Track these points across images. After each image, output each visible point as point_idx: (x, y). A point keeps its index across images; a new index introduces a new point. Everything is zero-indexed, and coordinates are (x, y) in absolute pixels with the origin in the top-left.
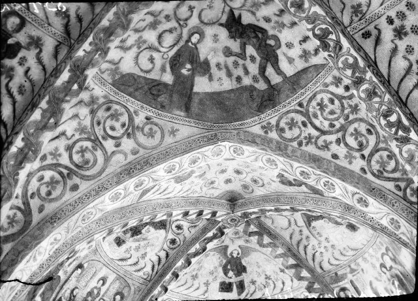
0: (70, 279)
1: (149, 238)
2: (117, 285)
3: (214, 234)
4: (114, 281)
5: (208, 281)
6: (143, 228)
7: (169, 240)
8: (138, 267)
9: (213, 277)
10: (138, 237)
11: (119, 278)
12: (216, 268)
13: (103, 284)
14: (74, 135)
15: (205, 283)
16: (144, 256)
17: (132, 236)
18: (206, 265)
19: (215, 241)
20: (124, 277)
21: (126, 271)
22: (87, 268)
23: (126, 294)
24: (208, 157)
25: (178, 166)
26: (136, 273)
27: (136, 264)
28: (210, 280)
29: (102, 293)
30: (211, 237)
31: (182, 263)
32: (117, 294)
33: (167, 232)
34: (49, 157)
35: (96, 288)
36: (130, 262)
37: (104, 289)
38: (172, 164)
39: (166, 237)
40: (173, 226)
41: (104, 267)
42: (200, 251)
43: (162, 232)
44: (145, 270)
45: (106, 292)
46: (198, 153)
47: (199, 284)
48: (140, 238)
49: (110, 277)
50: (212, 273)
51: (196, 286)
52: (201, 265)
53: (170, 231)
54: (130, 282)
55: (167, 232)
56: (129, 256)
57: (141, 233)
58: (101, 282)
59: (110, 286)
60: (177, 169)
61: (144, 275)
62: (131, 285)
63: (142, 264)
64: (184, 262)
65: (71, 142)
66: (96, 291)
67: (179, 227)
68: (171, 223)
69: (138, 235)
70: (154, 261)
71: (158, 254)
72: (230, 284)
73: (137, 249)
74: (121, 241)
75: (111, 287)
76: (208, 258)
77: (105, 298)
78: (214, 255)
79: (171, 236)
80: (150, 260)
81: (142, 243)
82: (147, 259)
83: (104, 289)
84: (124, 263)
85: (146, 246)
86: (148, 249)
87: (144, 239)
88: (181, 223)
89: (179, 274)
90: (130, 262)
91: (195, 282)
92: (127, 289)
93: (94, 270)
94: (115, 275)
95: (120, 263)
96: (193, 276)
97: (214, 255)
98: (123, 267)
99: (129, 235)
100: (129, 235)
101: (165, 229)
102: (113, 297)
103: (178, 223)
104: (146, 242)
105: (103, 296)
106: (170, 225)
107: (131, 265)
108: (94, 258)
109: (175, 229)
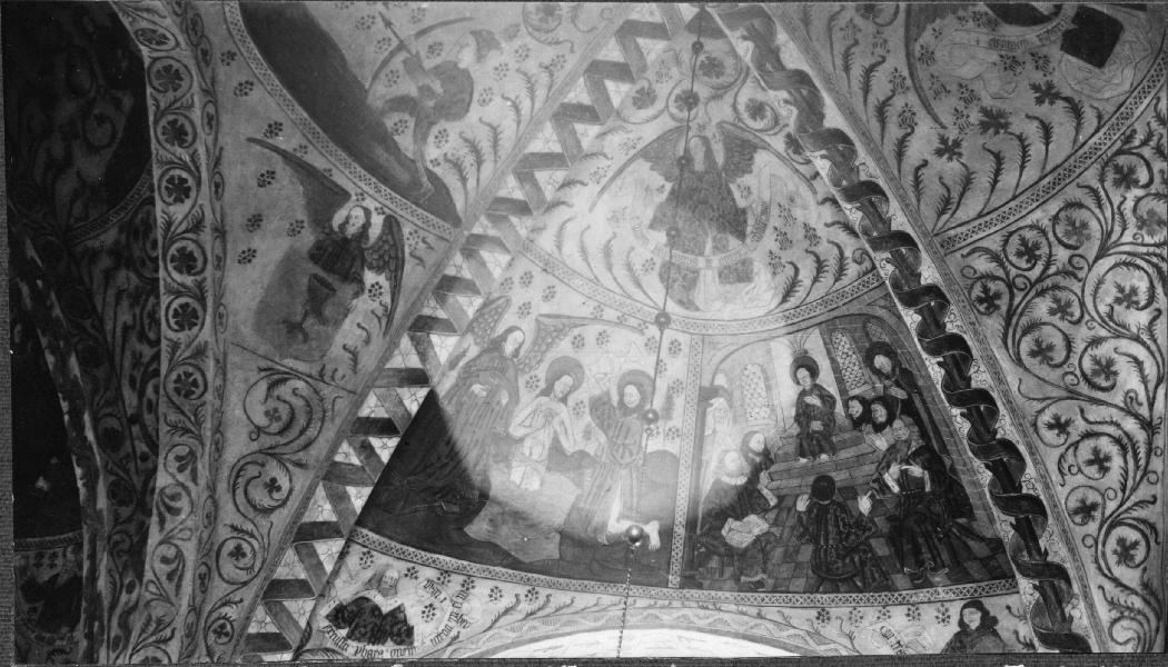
0: (708, 432)
1: (766, 196)
2: (844, 343)
3: (745, 38)
5: (1036, 88)
6: (733, 200)
7: (790, 151)
8: (832, 264)
9: (1030, 66)
10: (751, 221)
11: (829, 328)
12: (994, 44)
13: (814, 371)
14: (134, 315)
15: (1040, 101)
16: (811, 235)
18: (968, 71)
19: (782, 37)
20: (835, 313)
21: (824, 301)
22: (730, 380)
23: (886, 339)
24: (175, 101)
25: (177, 172)
26: (845, 280)
27: (820, 266)
28: (1039, 78)
29: (833, 390)
30: (757, 46)
31: (823, 157)
32: (868, 360)
33: (766, 147)
34: (135, 373)
35: (803, 394)
36: (806, 275)
37: (827, 379)
38: (164, 184)
39: (778, 155)
40: (751, 123)
41: (772, 344)
42: (804, 92)
43: (761, 158)
44: (848, 253)
45: (840, 380)
46: (156, 122)
47: (1028, 117)
48: (758, 221)
49: (807, 346)
50: (1011, 64)
51: (1032, 130)
52: (953, 88)
53: (767, 139)
54: (854, 309)
55: (766, 147)
56: (790, 271)
57: (744, 212)
58: (803, 373)
59: (833, 361)
60: (184, 175)
61: (860, 263)
62: (869, 311)
63: (825, 250)
64: (824, 152)
65: (138, 328)
66: (814, 400)
67: (757, 110)
68: (741, 124)
69: (745, 222)
70: (836, 219)
71: (820, 197)
73: (785, 241)
74: (740, 268)
75: (840, 361)
76: (938, 55)
77: (854, 392)
78: (938, 34)
79: (778, 143)
80: (827, 225)
81: (775, 220)
82: (822, 232)
83: (827, 379)
84: (800, 293)
85: (788, 217)
86: (798, 213)
87: (766, 210)
88: (743, 99)
89: (863, 177)
90: (806, 275)
91: (1015, 129)
92: (873, 328)
93: (757, 370)
94: (816, 332)
95: (793, 301)
96: (984, 127)
97: (938, 34)
98: (808, 300)
101: (755, 148)
102: (868, 372)
103: (741, 108)
104: (775, 211)
105: (843, 391)
106: (747, 129)
107: (816, 280)
108: (720, 355)
109: (759, 125)
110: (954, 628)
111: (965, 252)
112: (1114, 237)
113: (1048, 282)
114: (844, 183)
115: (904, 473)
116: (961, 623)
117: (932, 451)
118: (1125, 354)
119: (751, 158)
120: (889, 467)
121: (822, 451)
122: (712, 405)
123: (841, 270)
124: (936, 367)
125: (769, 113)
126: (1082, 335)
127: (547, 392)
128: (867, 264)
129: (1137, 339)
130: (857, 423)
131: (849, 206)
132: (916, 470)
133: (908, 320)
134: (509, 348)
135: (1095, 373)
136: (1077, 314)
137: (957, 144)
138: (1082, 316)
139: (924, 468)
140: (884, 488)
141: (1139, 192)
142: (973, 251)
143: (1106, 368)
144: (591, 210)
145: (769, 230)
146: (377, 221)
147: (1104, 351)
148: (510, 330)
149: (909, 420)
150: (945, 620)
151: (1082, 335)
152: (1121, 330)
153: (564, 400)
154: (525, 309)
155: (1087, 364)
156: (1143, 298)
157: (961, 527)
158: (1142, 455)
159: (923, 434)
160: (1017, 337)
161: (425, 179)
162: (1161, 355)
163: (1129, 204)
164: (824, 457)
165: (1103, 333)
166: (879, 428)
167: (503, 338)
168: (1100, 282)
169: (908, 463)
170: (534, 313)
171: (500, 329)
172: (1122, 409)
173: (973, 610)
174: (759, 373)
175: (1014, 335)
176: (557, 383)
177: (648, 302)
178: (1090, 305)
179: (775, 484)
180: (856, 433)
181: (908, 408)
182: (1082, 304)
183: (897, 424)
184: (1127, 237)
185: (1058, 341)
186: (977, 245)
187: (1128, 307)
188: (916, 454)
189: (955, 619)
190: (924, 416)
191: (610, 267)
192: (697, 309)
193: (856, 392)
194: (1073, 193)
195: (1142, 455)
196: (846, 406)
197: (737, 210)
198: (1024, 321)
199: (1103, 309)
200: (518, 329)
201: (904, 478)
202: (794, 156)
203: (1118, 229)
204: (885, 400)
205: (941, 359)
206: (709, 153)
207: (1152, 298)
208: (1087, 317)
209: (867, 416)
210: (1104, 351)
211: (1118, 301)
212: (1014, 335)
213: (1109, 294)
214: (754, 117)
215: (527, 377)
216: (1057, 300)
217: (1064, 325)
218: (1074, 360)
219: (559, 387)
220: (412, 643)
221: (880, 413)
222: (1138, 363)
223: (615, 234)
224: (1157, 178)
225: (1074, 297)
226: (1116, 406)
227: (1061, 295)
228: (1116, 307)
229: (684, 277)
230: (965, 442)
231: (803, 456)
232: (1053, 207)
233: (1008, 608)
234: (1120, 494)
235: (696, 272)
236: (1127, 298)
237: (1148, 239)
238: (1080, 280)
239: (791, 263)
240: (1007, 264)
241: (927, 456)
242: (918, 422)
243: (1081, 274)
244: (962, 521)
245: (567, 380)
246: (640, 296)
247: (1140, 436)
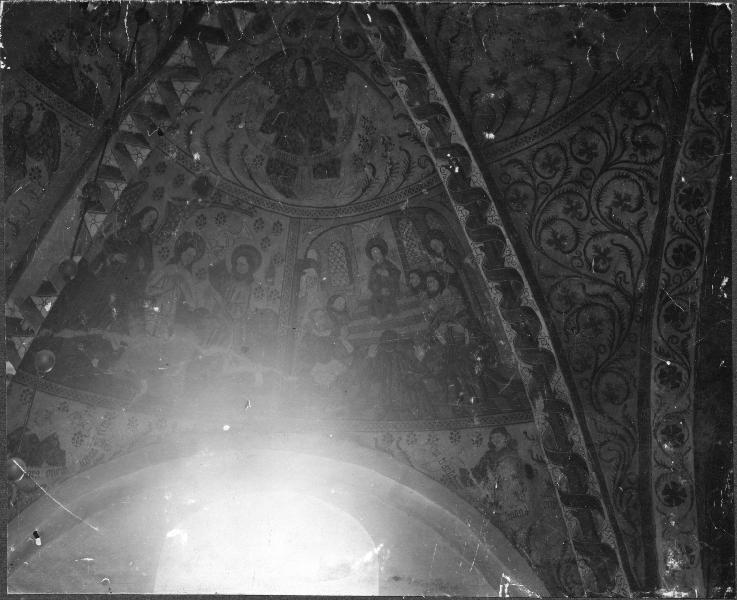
2: (407, 228)
4: (396, 228)
13: (384, 250)
17: (332, 139)
32: (426, 243)
35: (377, 267)
40: (347, 52)
43: (353, 78)
44: (415, 159)
58: (376, 251)
59: (399, 242)
81: (359, 131)
86: (379, 125)
87: (352, 120)
89: (432, 101)
90: (382, 176)
99: (326, 144)
100: (326, 144)
105: (405, 265)
110: (484, 448)
111: (505, 161)
112: (616, 156)
113: (565, 187)
114: (417, 104)
115: (450, 330)
116: (491, 445)
118: (617, 245)
119: (344, 78)
120: (439, 325)
121: (388, 312)
122: (305, 273)
123: (408, 171)
124: (479, 251)
125: (361, 44)
126: (587, 228)
127: (173, 261)
128: (430, 168)
129: (627, 233)
130: (415, 291)
131: (420, 122)
132: (459, 328)
133: (460, 215)
134: (145, 226)
136: (585, 214)
137: (504, 76)
138: (588, 215)
139: (466, 327)
140: (434, 342)
141: (638, 123)
142: (510, 162)
144: (215, 114)
145: (355, 134)
146: (39, 115)
147: (604, 242)
148: (147, 209)
150: (479, 441)
151: (587, 228)
152: (615, 226)
153: (189, 267)
154: (158, 194)
160: (539, 229)
161: (79, 83)
162: (645, 248)
164: (390, 316)
165: (603, 228)
166: (431, 295)
167: (141, 216)
168: (604, 188)
169: (453, 322)
170: (167, 197)
171: (138, 210)
172: (612, 286)
173: (500, 434)
174: (342, 251)
175: (537, 227)
176: (184, 254)
177: (260, 192)
178: (594, 208)
179: (351, 337)
180: (414, 298)
181: (454, 280)
183: (446, 291)
184: (625, 157)
185: (568, 231)
186: (513, 157)
187: (623, 210)
188: (460, 315)
189: (486, 441)
191: (228, 162)
192: (296, 198)
193: (416, 267)
196: (408, 277)
197: (330, 119)
198: (545, 217)
199: (604, 210)
200: (154, 209)
202: (379, 80)
204: (439, 279)
205: (482, 245)
206: (310, 76)
207: (641, 203)
208: (592, 216)
209: (423, 286)
211: (616, 204)
212: (537, 227)
213: (609, 199)
214: (347, 46)
215: (158, 248)
216: (569, 202)
217: (575, 222)
218: (581, 248)
219: (184, 256)
220: (64, 464)
221: (433, 285)
222: (628, 254)
223: (233, 134)
225: (582, 200)
226: (609, 284)
227: (575, 200)
228: (614, 209)
229: (286, 171)
230: (498, 307)
231: (374, 315)
232: (573, 130)
233: (525, 433)
234: (608, 349)
235: (296, 168)
236: (621, 201)
237: (641, 159)
238: (587, 188)
239: (370, 164)
240: (534, 173)
241: (467, 317)
243: (588, 184)
245: (192, 251)
246: (249, 183)
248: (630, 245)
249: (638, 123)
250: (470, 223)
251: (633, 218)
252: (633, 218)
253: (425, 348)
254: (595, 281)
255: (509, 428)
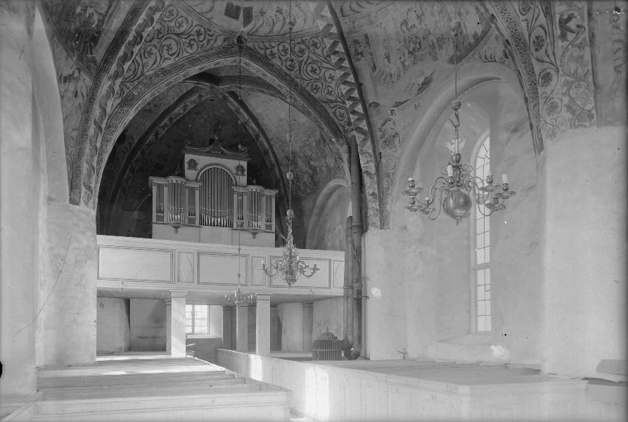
72: (238, 8)
113: (164, 24)
116: (73, 72)
117: (104, 20)
132: (96, 18)
135: (148, 52)
141: (196, 38)
143: (150, 53)
147: (155, 51)
149: (108, 4)
151: (155, 42)
155: (148, 49)
156: (171, 52)
157: (91, 45)
158: (136, 78)
159: (107, 12)
163: (192, 37)
182: (163, 37)
184: (184, 40)
188: (100, 14)
190: (112, 8)
194: (190, 19)
195: (136, 78)
199: (164, 44)
201: (91, 15)
203: (185, 37)
207: (172, 55)
210: (155, 51)
217: (155, 36)
218: (149, 44)
224: (202, 43)
236: (169, 48)
237: (186, 47)
242: (109, 7)
244: (92, 44)
247: (139, 74)
248: (158, 60)
249: (196, 38)
250: (150, 8)
251: (167, 56)
252: (167, 56)
253: (81, 10)
254: (141, 57)
255: (81, 73)
